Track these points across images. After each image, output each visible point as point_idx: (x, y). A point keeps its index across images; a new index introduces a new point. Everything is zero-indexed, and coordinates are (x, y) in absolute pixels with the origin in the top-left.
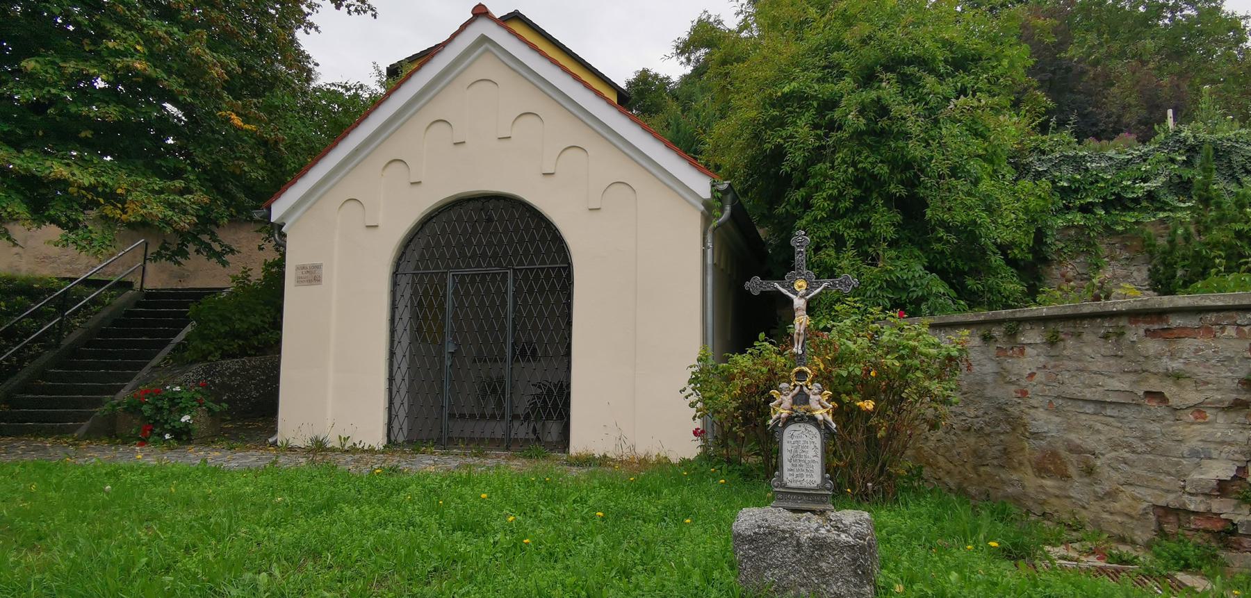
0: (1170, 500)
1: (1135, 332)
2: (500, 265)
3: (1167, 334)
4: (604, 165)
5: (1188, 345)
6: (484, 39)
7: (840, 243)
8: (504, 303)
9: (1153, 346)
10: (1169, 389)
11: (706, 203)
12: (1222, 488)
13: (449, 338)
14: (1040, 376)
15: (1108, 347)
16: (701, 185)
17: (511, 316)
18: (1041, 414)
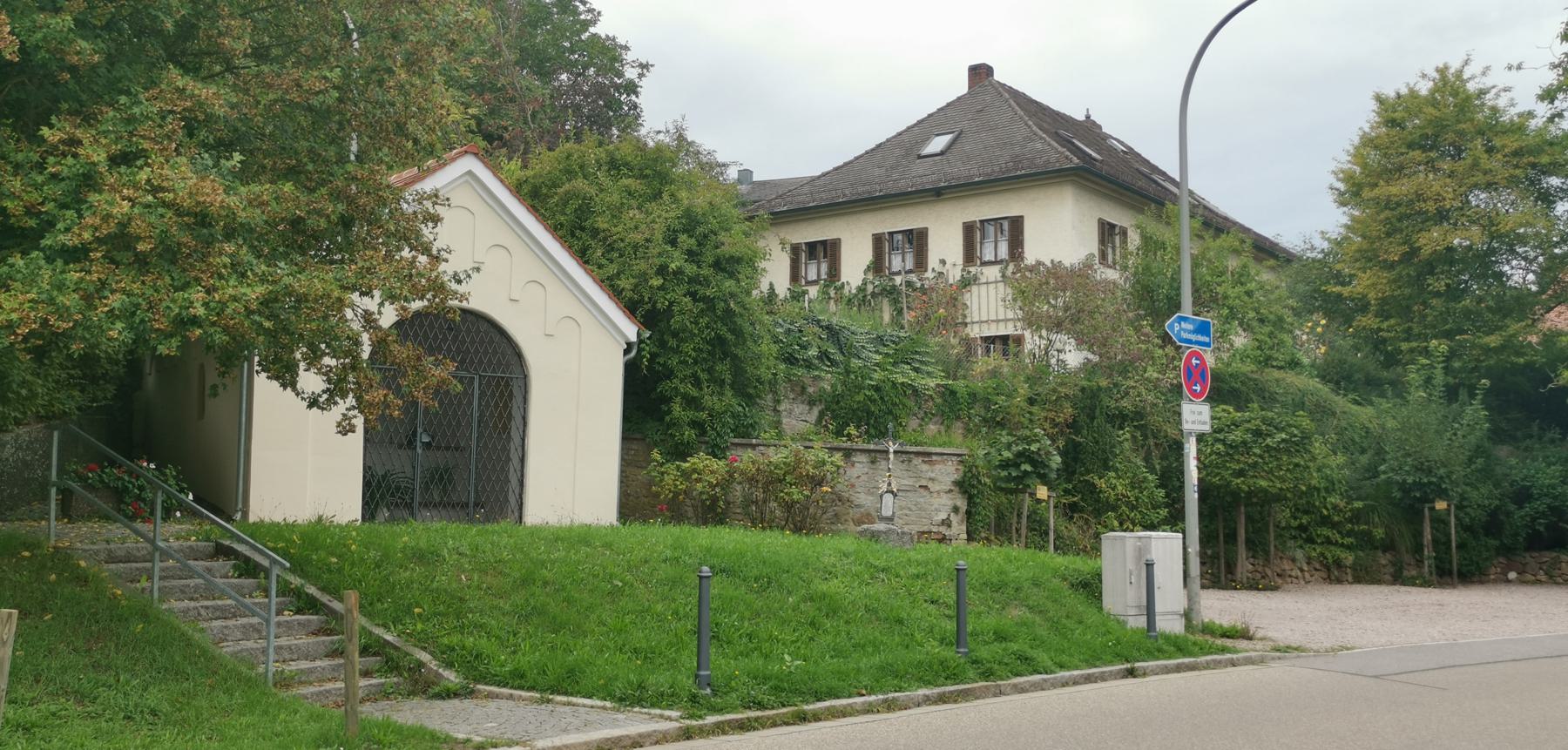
0: (925, 529)
1: (917, 461)
2: (467, 370)
3: (930, 463)
4: (561, 302)
5: (938, 467)
6: (470, 173)
7: (697, 383)
8: (470, 403)
9: (925, 467)
10: (930, 485)
11: (629, 345)
12: (943, 522)
13: (420, 430)
14: (864, 477)
15: (904, 466)
16: (631, 331)
17: (476, 415)
18: (862, 496)
